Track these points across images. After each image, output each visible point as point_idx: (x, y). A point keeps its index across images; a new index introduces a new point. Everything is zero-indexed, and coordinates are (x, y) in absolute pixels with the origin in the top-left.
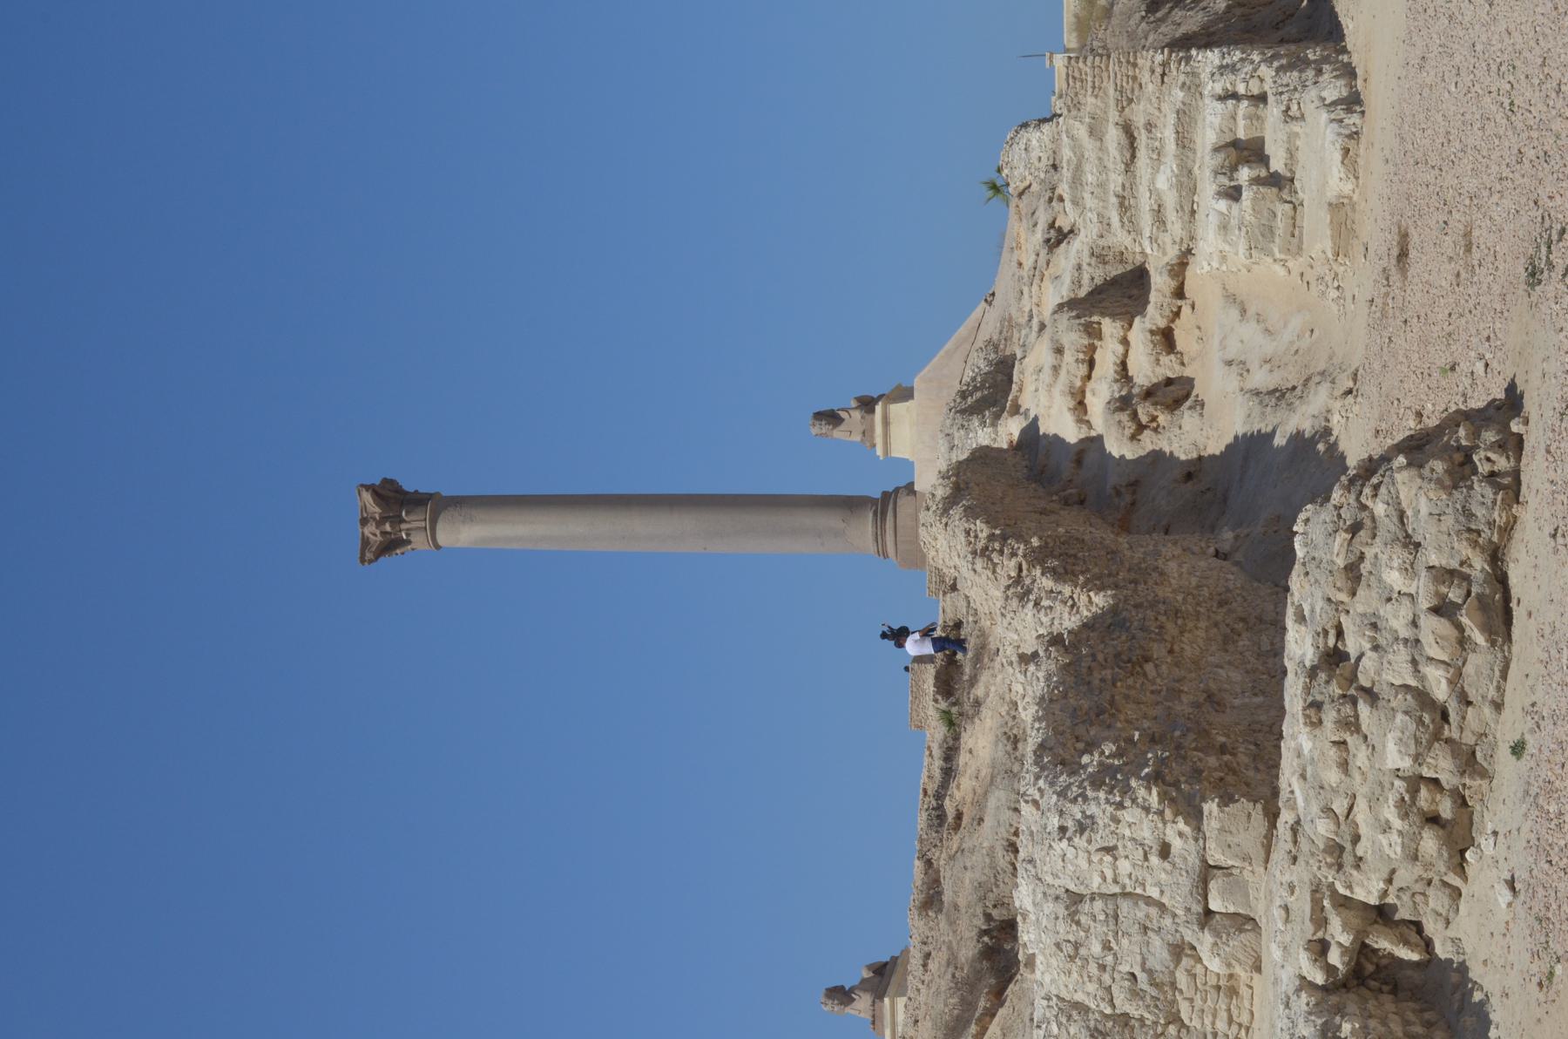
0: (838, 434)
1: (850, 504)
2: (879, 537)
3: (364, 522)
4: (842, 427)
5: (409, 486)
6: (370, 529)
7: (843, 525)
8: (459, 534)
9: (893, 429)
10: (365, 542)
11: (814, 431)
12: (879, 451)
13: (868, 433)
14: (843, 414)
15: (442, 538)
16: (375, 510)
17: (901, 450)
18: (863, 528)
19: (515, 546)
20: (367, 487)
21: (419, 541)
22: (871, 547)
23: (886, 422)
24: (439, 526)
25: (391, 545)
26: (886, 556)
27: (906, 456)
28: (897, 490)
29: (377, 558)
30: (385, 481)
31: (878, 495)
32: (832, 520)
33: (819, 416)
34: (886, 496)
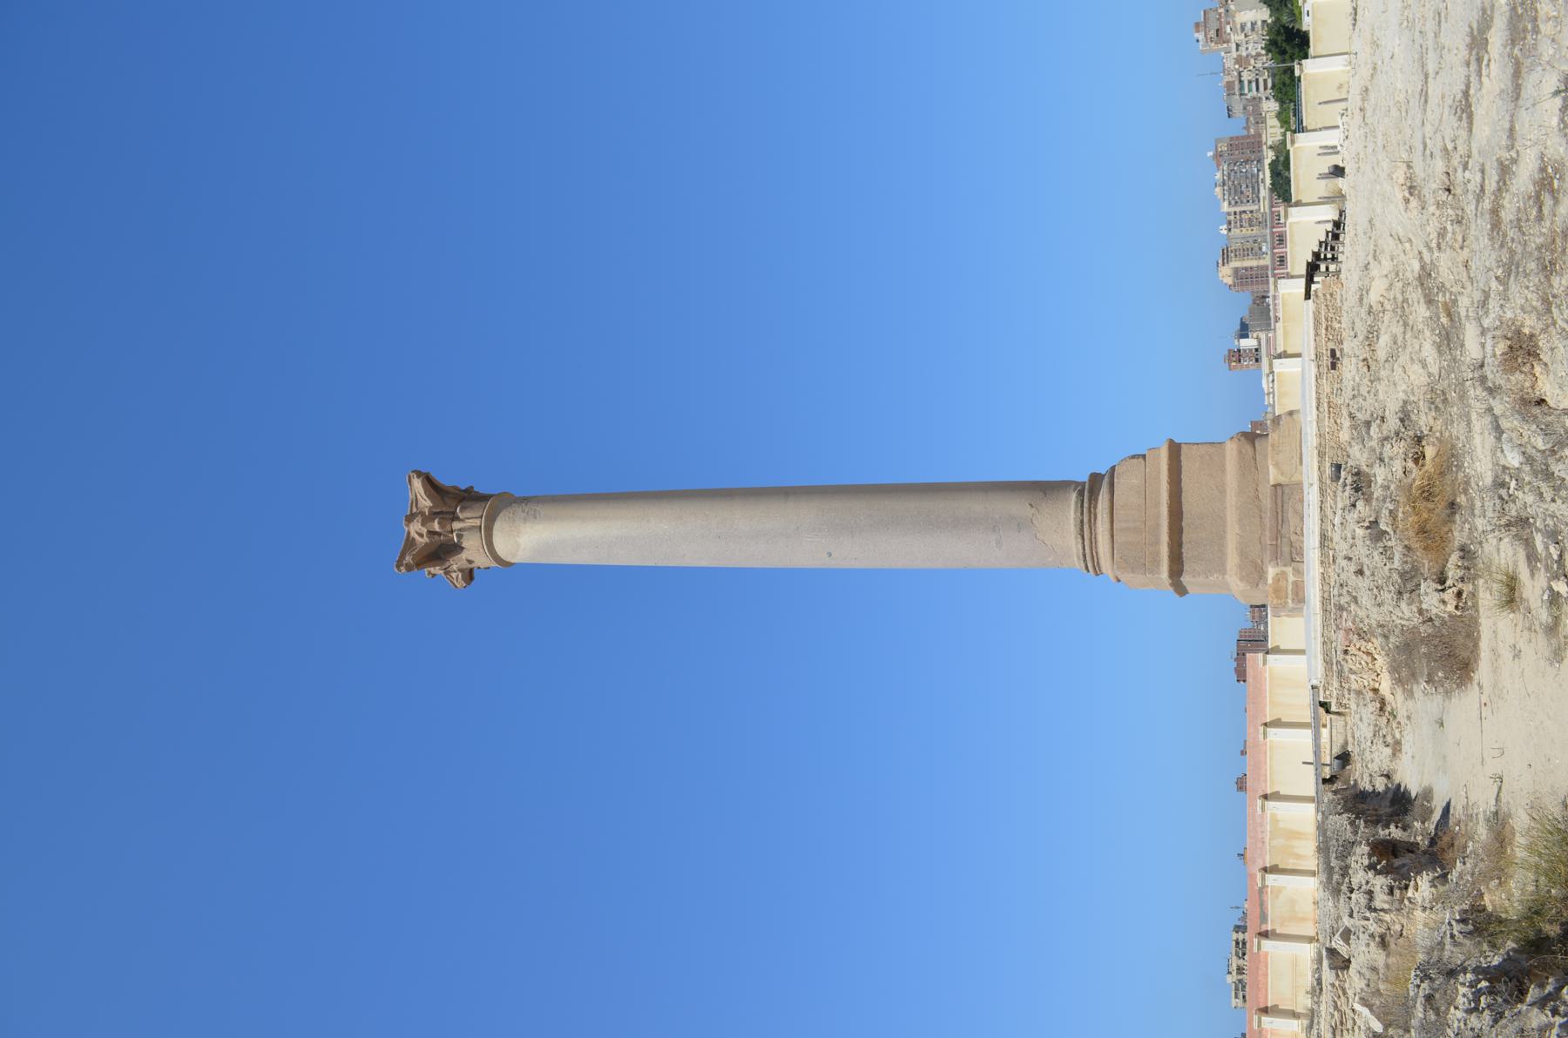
2: (1086, 529)
3: (410, 518)
5: (480, 488)
6: (416, 528)
7: (1029, 511)
8: (525, 540)
10: (410, 543)
16: (426, 503)
18: (1059, 525)
20: (419, 474)
22: (1072, 543)
25: (441, 552)
26: (1098, 571)
31: (1085, 478)
32: (1017, 506)
34: (1096, 479)
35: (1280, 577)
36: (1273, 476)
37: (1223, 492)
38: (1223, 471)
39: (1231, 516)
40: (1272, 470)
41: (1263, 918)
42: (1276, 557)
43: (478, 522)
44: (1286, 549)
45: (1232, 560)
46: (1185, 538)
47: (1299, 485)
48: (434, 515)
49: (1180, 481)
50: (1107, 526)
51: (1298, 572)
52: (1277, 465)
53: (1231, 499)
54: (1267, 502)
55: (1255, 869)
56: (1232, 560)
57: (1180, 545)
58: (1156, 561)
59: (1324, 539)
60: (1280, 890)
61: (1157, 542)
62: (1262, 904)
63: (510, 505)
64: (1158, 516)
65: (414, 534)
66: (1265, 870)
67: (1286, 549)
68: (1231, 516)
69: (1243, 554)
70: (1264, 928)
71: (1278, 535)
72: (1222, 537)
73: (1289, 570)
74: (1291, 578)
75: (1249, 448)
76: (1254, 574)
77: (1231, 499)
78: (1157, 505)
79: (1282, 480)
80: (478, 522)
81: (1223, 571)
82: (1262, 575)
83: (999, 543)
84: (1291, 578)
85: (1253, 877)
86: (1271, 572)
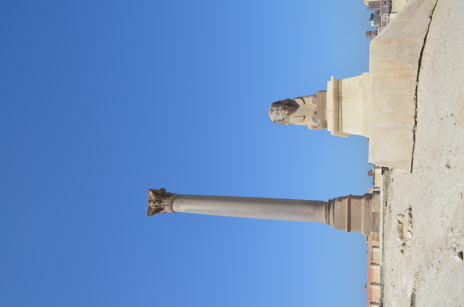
0: (294, 119)
1: (316, 204)
2: (327, 217)
3: (150, 201)
4: (298, 113)
5: (167, 191)
6: (151, 204)
7: (313, 211)
8: (181, 208)
9: (345, 103)
10: (150, 208)
11: (273, 116)
12: (331, 127)
13: (320, 113)
14: (299, 102)
15: (175, 208)
16: (153, 198)
17: (353, 126)
19: (198, 213)
20: (151, 190)
21: (167, 209)
22: (324, 220)
23: (338, 98)
24: (174, 204)
25: (158, 210)
26: (329, 224)
27: (360, 134)
28: (334, 199)
29: (153, 214)
30: (162, 189)
32: (309, 210)
33: (277, 104)
34: (330, 201)
35: (374, 235)
36: (373, 210)
37: (361, 211)
38: (361, 206)
39: (363, 218)
40: (373, 209)
41: (372, 259)
42: (373, 230)
43: (168, 203)
44: (375, 228)
45: (362, 229)
46: (351, 222)
47: (379, 213)
48: (156, 201)
49: (350, 208)
50: (332, 215)
51: (378, 234)
52: (374, 208)
53: (363, 214)
54: (371, 216)
55: (370, 247)
56: (362, 229)
57: (350, 224)
58: (344, 227)
59: (383, 234)
60: (377, 252)
61: (345, 223)
62: (372, 256)
63: (176, 198)
64: (345, 216)
65: (151, 206)
66: (373, 247)
67: (375, 228)
68: (363, 218)
69: (365, 228)
70: (372, 262)
71: (373, 225)
72: (360, 222)
73: (376, 233)
74: (376, 235)
75: (367, 202)
76: (368, 233)
77: (363, 214)
78: (345, 213)
79: (375, 212)
80: (168, 203)
81: (360, 231)
82: (369, 234)
83: (305, 218)
84: (376, 235)
85: (370, 248)
86: (372, 233)
